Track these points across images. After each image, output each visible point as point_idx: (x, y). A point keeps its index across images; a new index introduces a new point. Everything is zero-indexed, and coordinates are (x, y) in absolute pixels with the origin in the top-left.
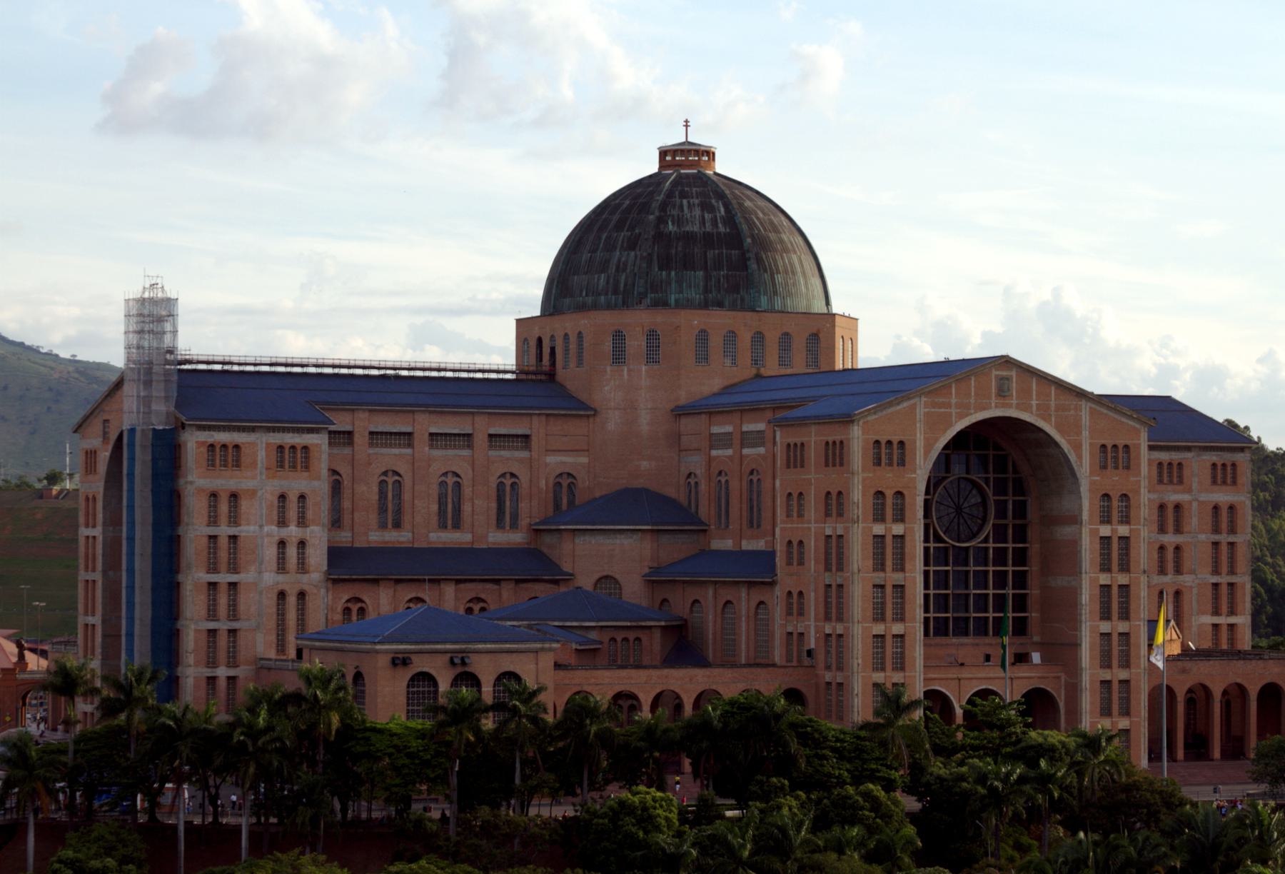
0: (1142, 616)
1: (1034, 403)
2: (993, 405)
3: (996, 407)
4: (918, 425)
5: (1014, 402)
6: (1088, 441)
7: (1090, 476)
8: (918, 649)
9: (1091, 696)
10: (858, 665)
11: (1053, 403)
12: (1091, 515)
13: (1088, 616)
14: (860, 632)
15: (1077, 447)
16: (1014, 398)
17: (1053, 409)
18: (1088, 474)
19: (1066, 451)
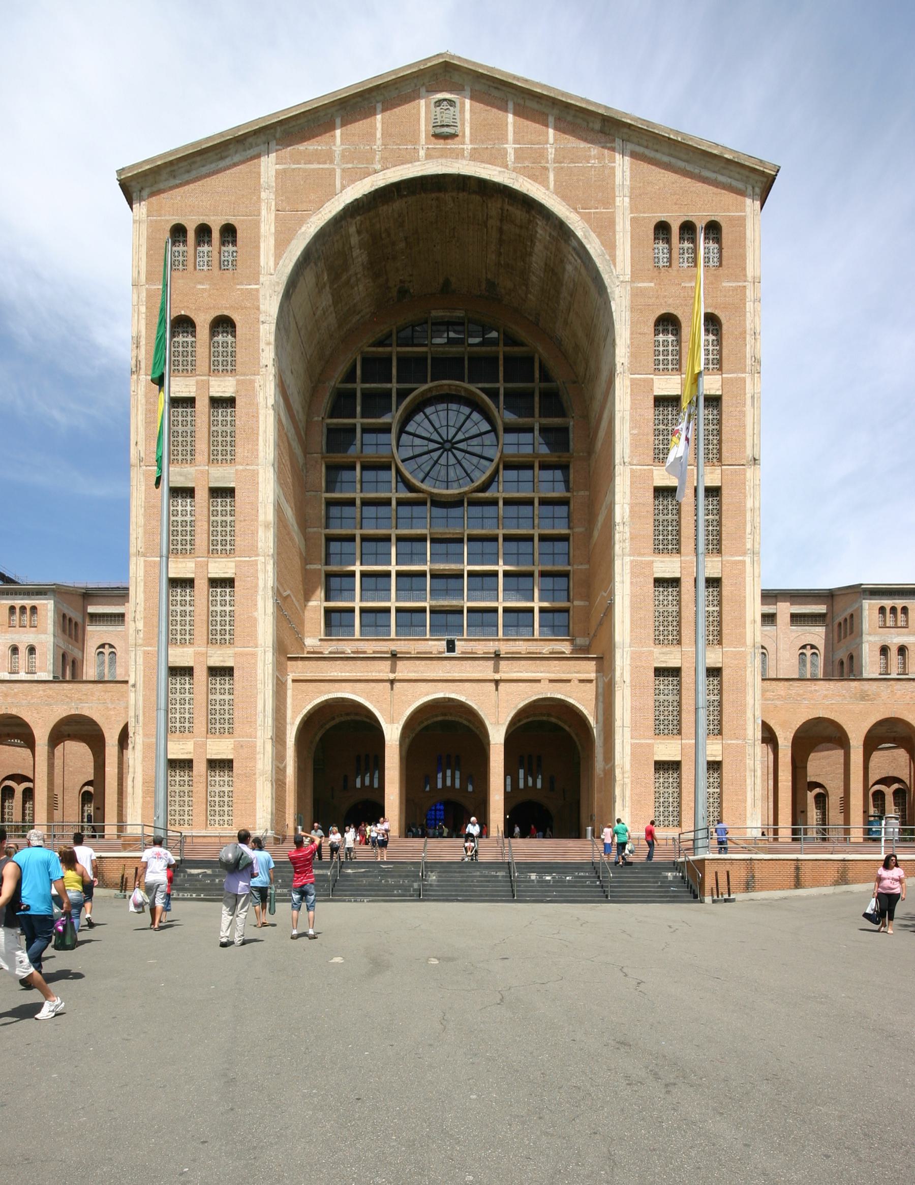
0: (749, 546)
1: (510, 148)
2: (422, 153)
3: (428, 157)
4: (263, 195)
5: (468, 147)
6: (628, 217)
7: (632, 281)
8: (260, 604)
9: (633, 695)
10: (138, 631)
11: (551, 152)
12: (634, 355)
13: (627, 544)
14: (141, 573)
15: (605, 229)
16: (467, 140)
17: (551, 157)
18: (628, 278)
19: (579, 234)
